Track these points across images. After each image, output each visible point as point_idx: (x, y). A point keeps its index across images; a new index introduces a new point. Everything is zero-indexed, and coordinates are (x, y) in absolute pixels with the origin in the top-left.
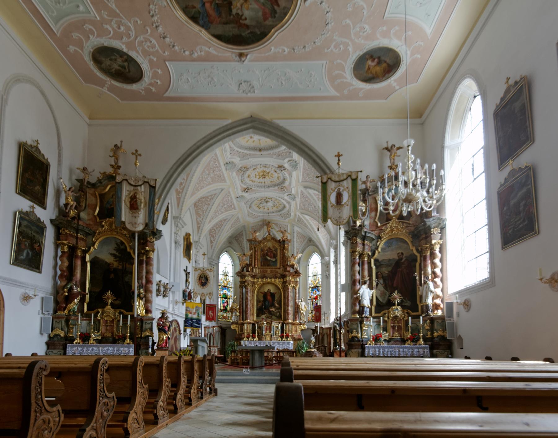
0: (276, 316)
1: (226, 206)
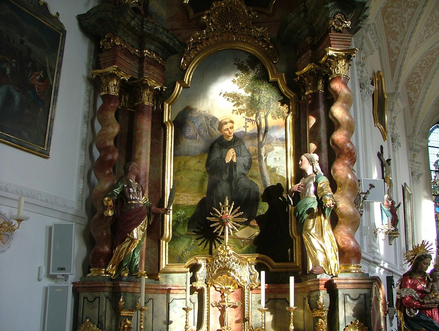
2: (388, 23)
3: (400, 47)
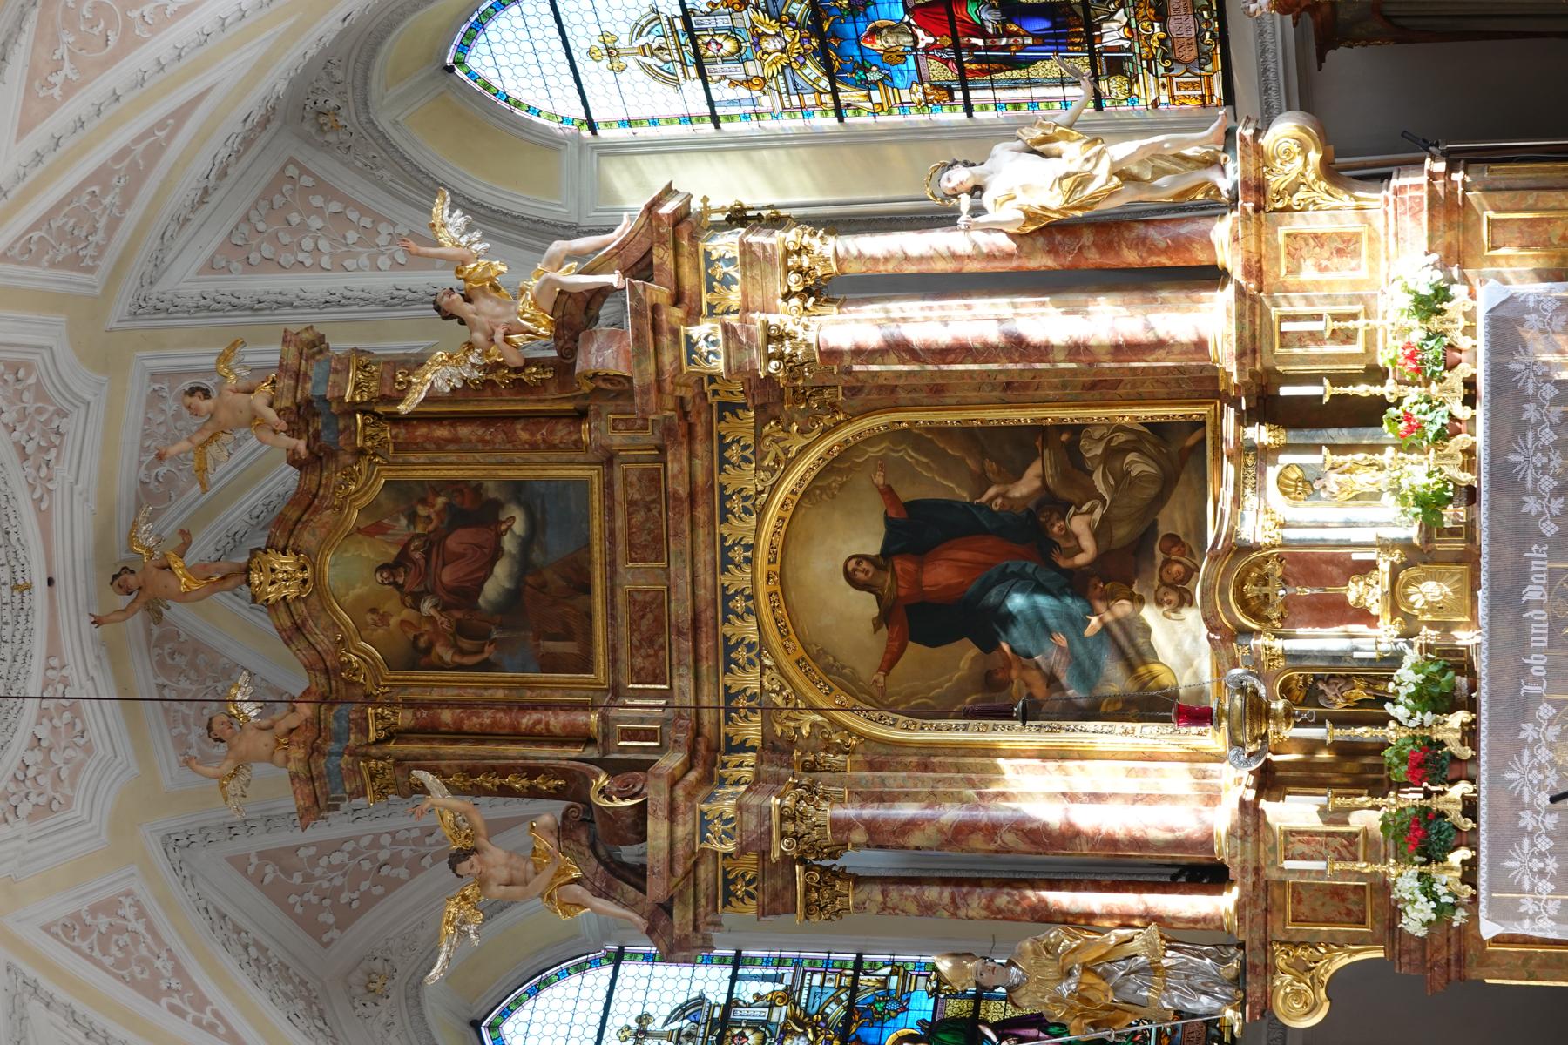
0: (1167, 484)
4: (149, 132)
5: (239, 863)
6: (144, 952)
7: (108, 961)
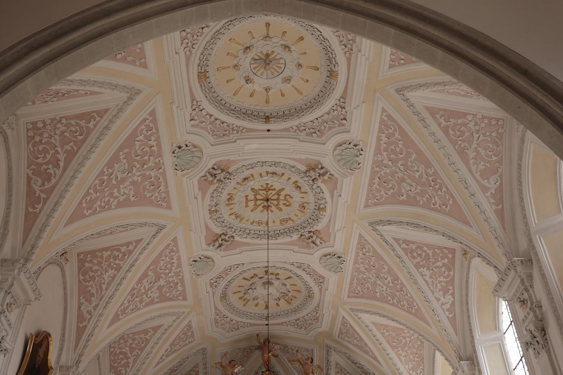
1: (162, 282)
2: (83, 280)
3: (93, 311)
4: (371, 351)
5: (197, 366)
6: (181, 343)
7: (181, 335)
